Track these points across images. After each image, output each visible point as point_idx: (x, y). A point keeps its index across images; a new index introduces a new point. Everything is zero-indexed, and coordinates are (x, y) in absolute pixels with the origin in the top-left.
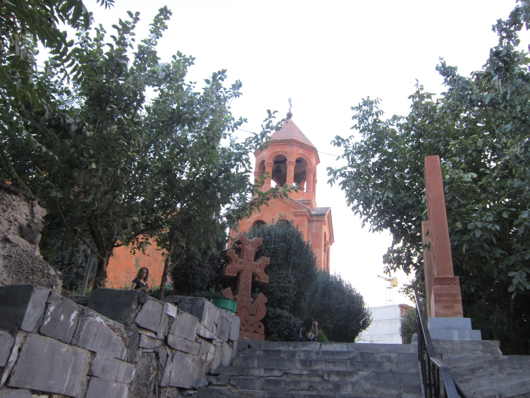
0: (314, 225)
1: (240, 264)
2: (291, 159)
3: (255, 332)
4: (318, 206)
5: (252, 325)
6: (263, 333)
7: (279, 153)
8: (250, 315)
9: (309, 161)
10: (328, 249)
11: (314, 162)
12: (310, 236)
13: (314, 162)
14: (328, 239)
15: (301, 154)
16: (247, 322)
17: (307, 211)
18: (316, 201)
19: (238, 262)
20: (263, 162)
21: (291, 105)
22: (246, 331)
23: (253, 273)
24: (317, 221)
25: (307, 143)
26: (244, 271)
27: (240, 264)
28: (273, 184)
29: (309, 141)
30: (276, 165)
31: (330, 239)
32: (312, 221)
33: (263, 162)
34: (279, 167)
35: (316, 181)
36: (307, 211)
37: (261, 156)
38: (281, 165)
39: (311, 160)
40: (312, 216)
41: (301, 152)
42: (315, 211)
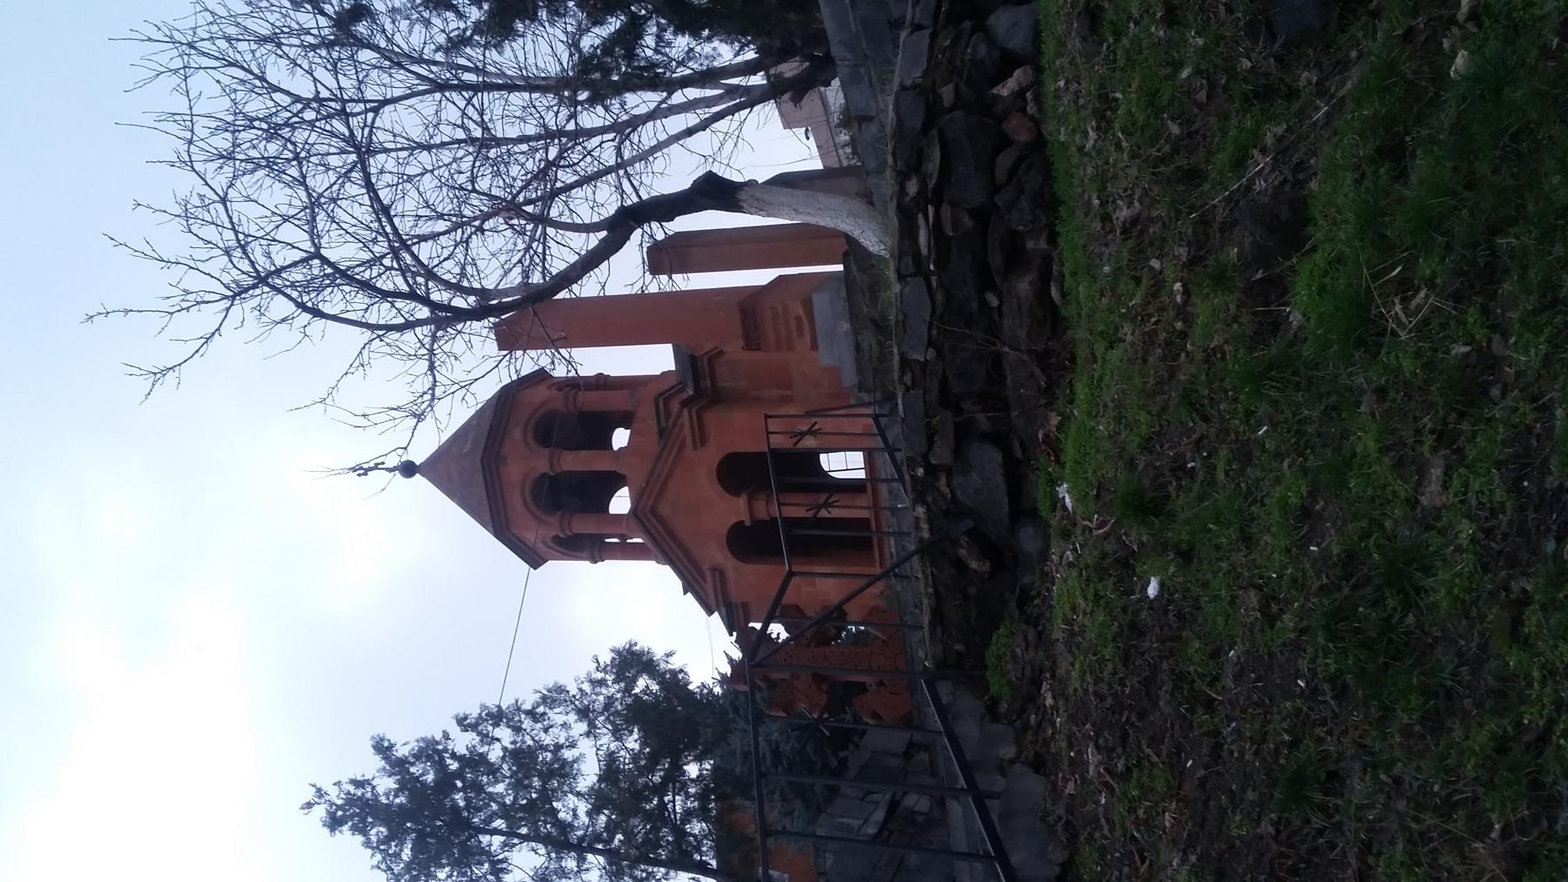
2: (541, 463)
4: (673, 368)
9: (542, 405)
11: (541, 393)
15: (525, 431)
17: (685, 412)
20: (556, 539)
21: (376, 467)
25: (489, 414)
28: (621, 503)
33: (556, 539)
36: (685, 412)
37: (541, 547)
41: (517, 433)
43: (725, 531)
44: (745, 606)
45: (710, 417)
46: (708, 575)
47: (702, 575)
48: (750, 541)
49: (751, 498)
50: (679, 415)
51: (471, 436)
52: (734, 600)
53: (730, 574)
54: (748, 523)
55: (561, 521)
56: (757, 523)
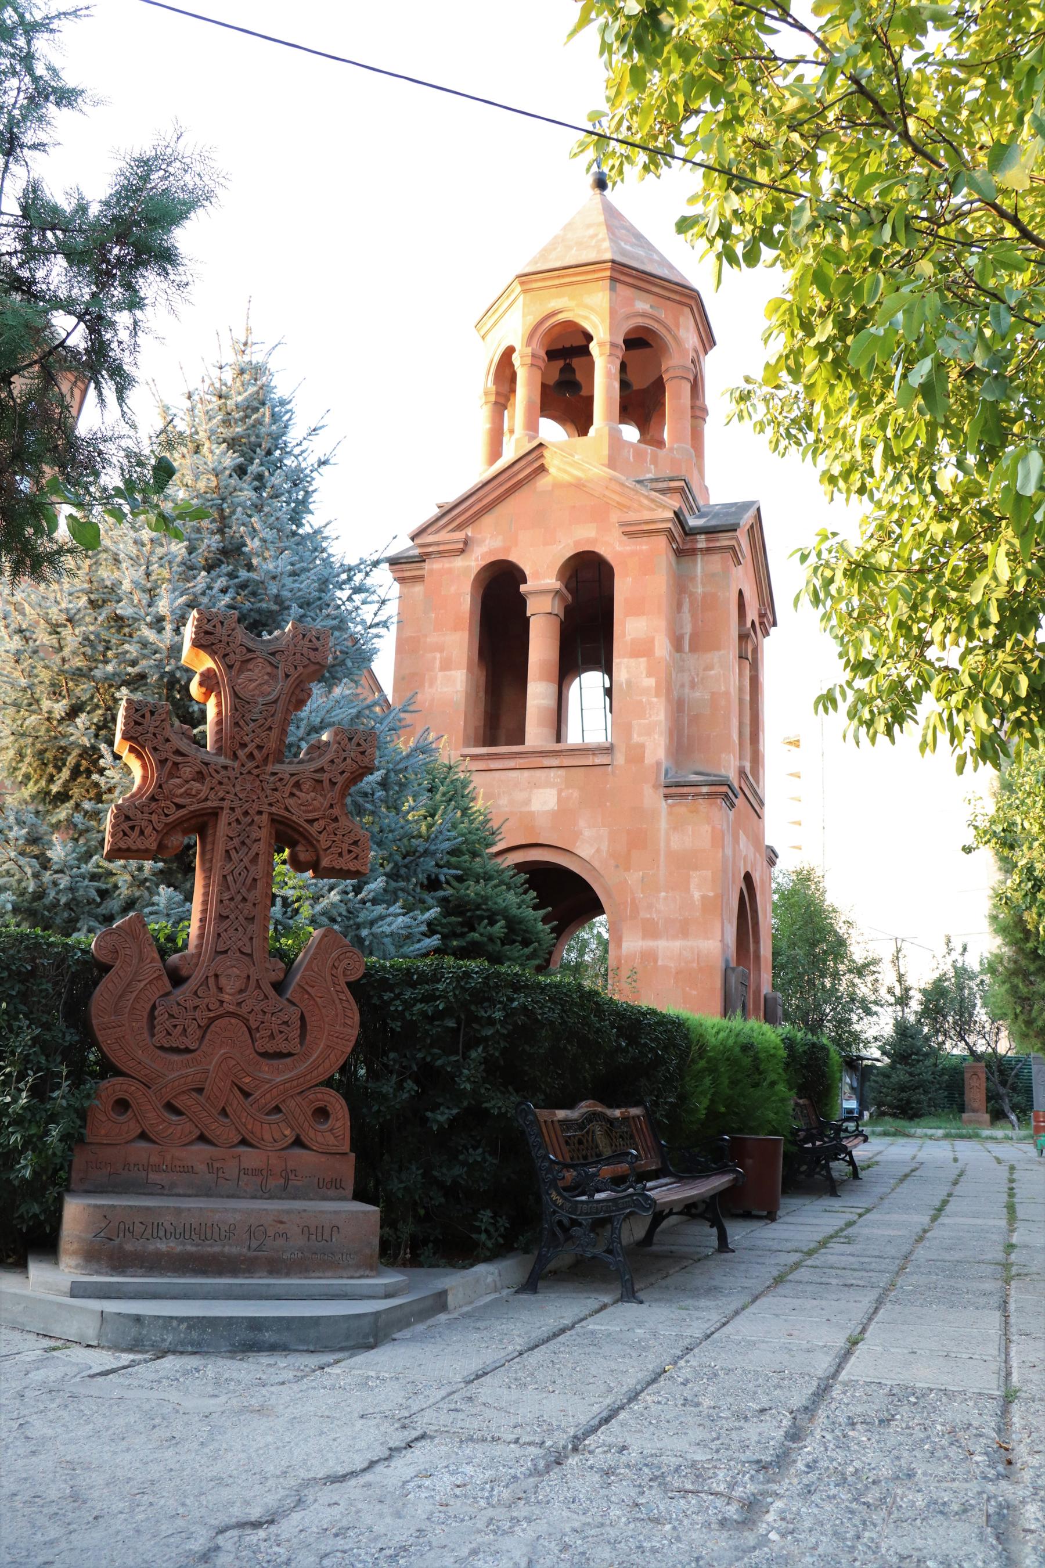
0: (700, 566)
1: (200, 777)
3: (298, 1143)
4: (712, 503)
5: (277, 1109)
6: (346, 1148)
7: (562, 317)
8: (265, 1055)
9: (676, 338)
10: (755, 650)
12: (686, 607)
13: (690, 338)
14: (752, 615)
15: (644, 315)
16: (247, 1095)
18: (708, 482)
19: (187, 772)
22: (244, 1142)
23: (274, 820)
24: (708, 550)
26: (224, 818)
27: (200, 777)
29: (671, 267)
30: (560, 364)
31: (762, 616)
32: (693, 552)
33: (510, 351)
34: (568, 369)
35: (705, 410)
38: (576, 362)
39: (682, 333)
40: (689, 533)
41: (642, 304)
42: (702, 516)
43: (510, 559)
44: (420, 578)
45: (662, 541)
46: (460, 535)
47: (459, 527)
48: (500, 593)
49: (557, 592)
50: (664, 507)
51: (641, 252)
52: (427, 565)
53: (459, 562)
54: (523, 588)
56: (521, 602)
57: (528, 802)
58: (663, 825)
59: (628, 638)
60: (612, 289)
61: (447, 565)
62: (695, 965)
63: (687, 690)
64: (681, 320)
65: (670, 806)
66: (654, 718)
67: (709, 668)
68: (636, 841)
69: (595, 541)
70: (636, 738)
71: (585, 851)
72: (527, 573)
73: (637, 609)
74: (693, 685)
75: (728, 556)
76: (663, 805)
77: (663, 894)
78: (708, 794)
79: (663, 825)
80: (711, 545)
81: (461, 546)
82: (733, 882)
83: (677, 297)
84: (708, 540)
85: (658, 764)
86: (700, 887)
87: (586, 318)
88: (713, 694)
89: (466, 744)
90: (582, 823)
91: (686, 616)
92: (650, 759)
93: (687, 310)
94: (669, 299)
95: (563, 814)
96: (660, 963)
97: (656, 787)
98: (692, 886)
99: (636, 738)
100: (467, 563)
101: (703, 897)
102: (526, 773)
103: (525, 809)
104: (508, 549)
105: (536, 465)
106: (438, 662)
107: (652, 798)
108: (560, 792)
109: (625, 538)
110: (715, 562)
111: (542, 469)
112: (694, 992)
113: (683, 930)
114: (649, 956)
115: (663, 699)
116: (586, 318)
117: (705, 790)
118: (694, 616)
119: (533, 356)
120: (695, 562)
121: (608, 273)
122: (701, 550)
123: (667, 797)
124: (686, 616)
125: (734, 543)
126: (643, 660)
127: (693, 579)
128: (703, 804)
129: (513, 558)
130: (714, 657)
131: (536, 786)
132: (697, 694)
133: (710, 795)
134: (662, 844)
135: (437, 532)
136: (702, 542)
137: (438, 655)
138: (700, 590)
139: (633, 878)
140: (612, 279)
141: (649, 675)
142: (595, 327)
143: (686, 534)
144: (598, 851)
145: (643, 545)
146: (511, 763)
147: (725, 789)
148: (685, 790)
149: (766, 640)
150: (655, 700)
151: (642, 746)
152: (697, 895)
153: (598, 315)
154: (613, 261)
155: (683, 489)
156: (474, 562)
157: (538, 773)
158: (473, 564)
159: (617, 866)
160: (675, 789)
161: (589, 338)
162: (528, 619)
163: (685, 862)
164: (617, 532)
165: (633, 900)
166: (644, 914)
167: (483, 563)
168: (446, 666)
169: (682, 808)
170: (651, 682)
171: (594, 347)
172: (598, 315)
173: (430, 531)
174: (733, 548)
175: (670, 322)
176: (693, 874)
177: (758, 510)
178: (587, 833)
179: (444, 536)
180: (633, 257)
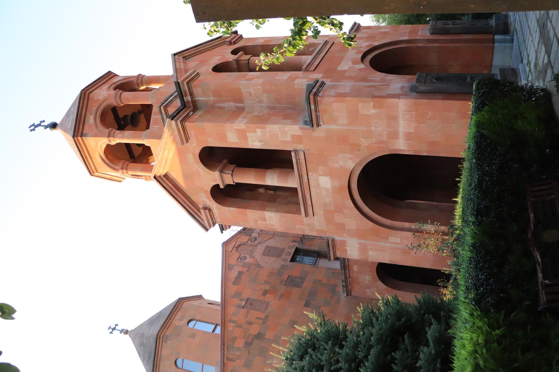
0: (200, 98)
9: (104, 101)
12: (222, 105)
15: (95, 119)
21: (39, 125)
24: (191, 94)
25: (76, 107)
29: (75, 102)
32: (194, 102)
39: (101, 98)
40: (184, 105)
41: (91, 119)
43: (210, 191)
45: (188, 124)
46: (202, 211)
49: (221, 172)
54: (222, 187)
55: (124, 163)
56: (228, 186)
57: (327, 190)
58: (334, 127)
59: (238, 141)
60: (86, 136)
61: (217, 216)
62: (414, 113)
63: (263, 105)
64: (95, 98)
65: (324, 123)
66: (277, 130)
67: (250, 94)
68: (344, 141)
69: (194, 154)
70: (289, 139)
71: (351, 165)
72: (215, 184)
73: (223, 137)
74: (261, 102)
75: (193, 84)
76: (323, 127)
77: (373, 128)
78: (315, 105)
79: (334, 127)
80: (188, 94)
81: (207, 211)
82: (365, 79)
83: (86, 101)
84: (186, 96)
85: (301, 128)
86: (368, 108)
87: (101, 147)
88: (263, 92)
89: (300, 213)
90: (336, 166)
91: (226, 105)
92: (299, 133)
93: (91, 95)
94: (87, 105)
95: (331, 174)
96: (412, 131)
97: (314, 131)
98: (368, 113)
99: (289, 139)
100: (215, 208)
101: (374, 107)
102: (312, 189)
103: (331, 191)
104: (205, 191)
105: (165, 179)
106: (263, 222)
107: (319, 132)
108: (320, 175)
109: (190, 141)
110: (197, 91)
111: (166, 176)
112: (430, 113)
113: (393, 118)
114: (409, 136)
115: (267, 125)
116: (101, 147)
117: (313, 107)
118: (225, 101)
119: (122, 169)
120: (198, 100)
121: (79, 138)
122: (192, 98)
123: (318, 125)
124: (226, 105)
125: (185, 83)
126: (248, 134)
127: (207, 102)
128: (321, 107)
129: (209, 190)
130: (244, 91)
131: (318, 185)
132: (265, 100)
133: (316, 103)
134: (345, 128)
135: (203, 220)
136: (188, 98)
137: (259, 222)
138: (212, 98)
139: (364, 143)
140: (81, 136)
141: (255, 132)
142: (104, 143)
143: (185, 106)
144: (350, 159)
145: (191, 133)
146: (308, 196)
147: (311, 97)
148: (314, 117)
149: (244, 36)
150: (267, 129)
151: (293, 136)
152: (373, 111)
153: (98, 144)
154: (73, 137)
155: (165, 107)
156: (213, 205)
157: (311, 184)
158: (215, 205)
159: (358, 150)
160: (313, 121)
161: (108, 146)
162: (237, 183)
163: (354, 116)
164: (188, 145)
165: (376, 143)
166: (385, 138)
167: (214, 201)
168: (265, 220)
169: (324, 118)
170: (259, 131)
171: (113, 143)
172: (98, 144)
173: (203, 223)
174: (188, 83)
175: (97, 105)
176: (361, 113)
177: (175, 55)
178: (341, 163)
179: (203, 217)
180: (72, 123)
